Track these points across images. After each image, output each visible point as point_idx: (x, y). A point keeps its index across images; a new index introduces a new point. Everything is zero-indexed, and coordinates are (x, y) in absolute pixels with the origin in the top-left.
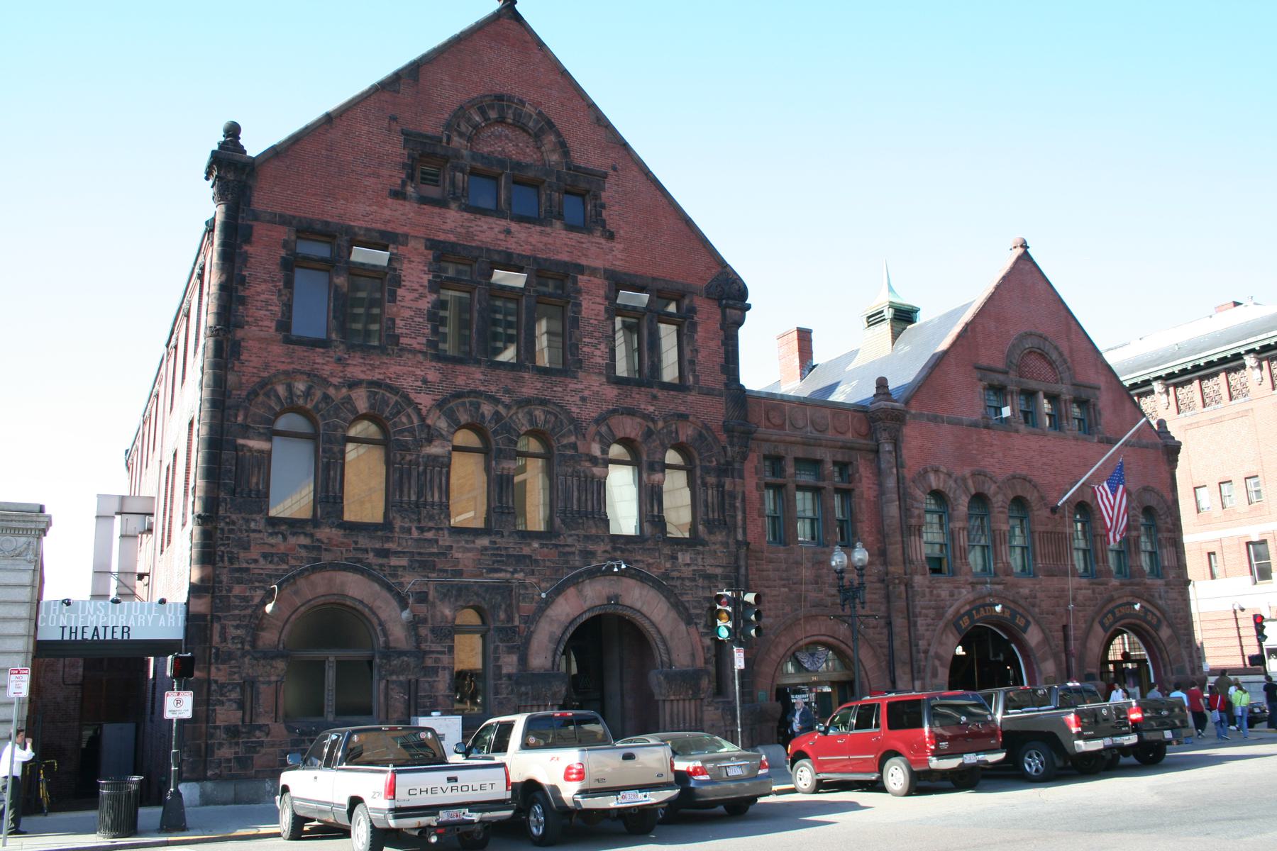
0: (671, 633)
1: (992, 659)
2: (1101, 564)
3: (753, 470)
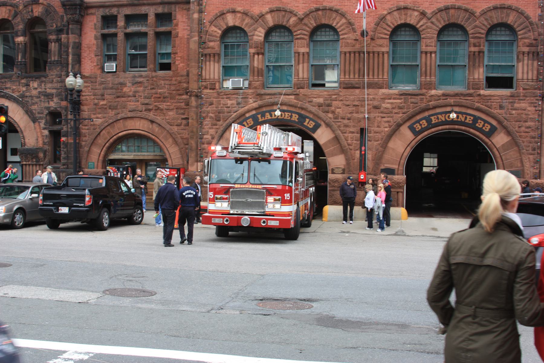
0: (25, 127)
2: (428, 78)
3: (93, 27)
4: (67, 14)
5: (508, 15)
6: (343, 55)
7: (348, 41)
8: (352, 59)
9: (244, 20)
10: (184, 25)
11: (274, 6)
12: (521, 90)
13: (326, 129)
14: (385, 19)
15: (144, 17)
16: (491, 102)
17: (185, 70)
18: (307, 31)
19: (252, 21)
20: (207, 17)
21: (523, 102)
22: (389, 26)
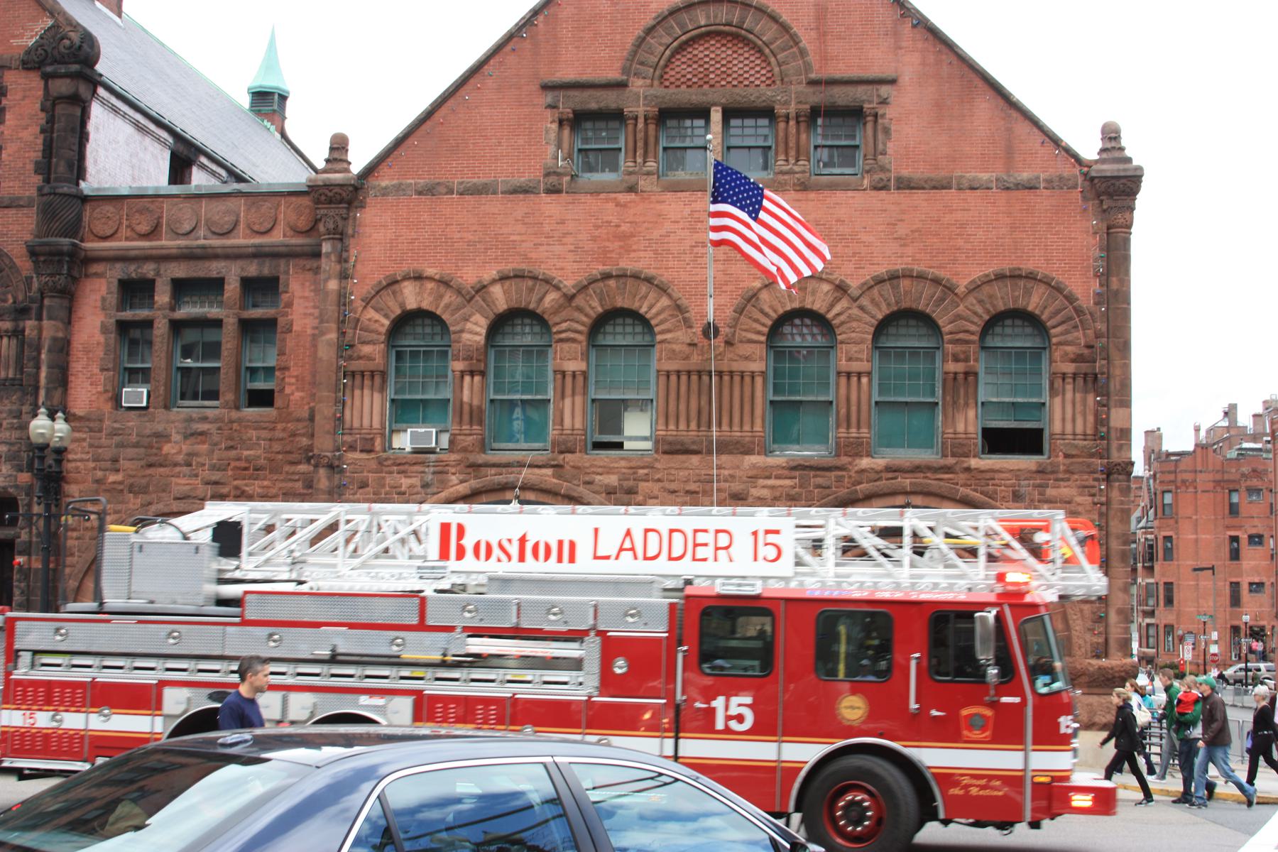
2: (853, 430)
3: (99, 304)
4: (39, 274)
5: (1028, 293)
6: (663, 379)
7: (674, 346)
8: (683, 388)
9: (441, 297)
10: (307, 304)
11: (509, 267)
12: (1061, 459)
15: (216, 285)
16: (993, 485)
17: (306, 407)
18: (583, 324)
19: (460, 299)
20: (358, 289)
21: (1066, 484)
22: (766, 315)
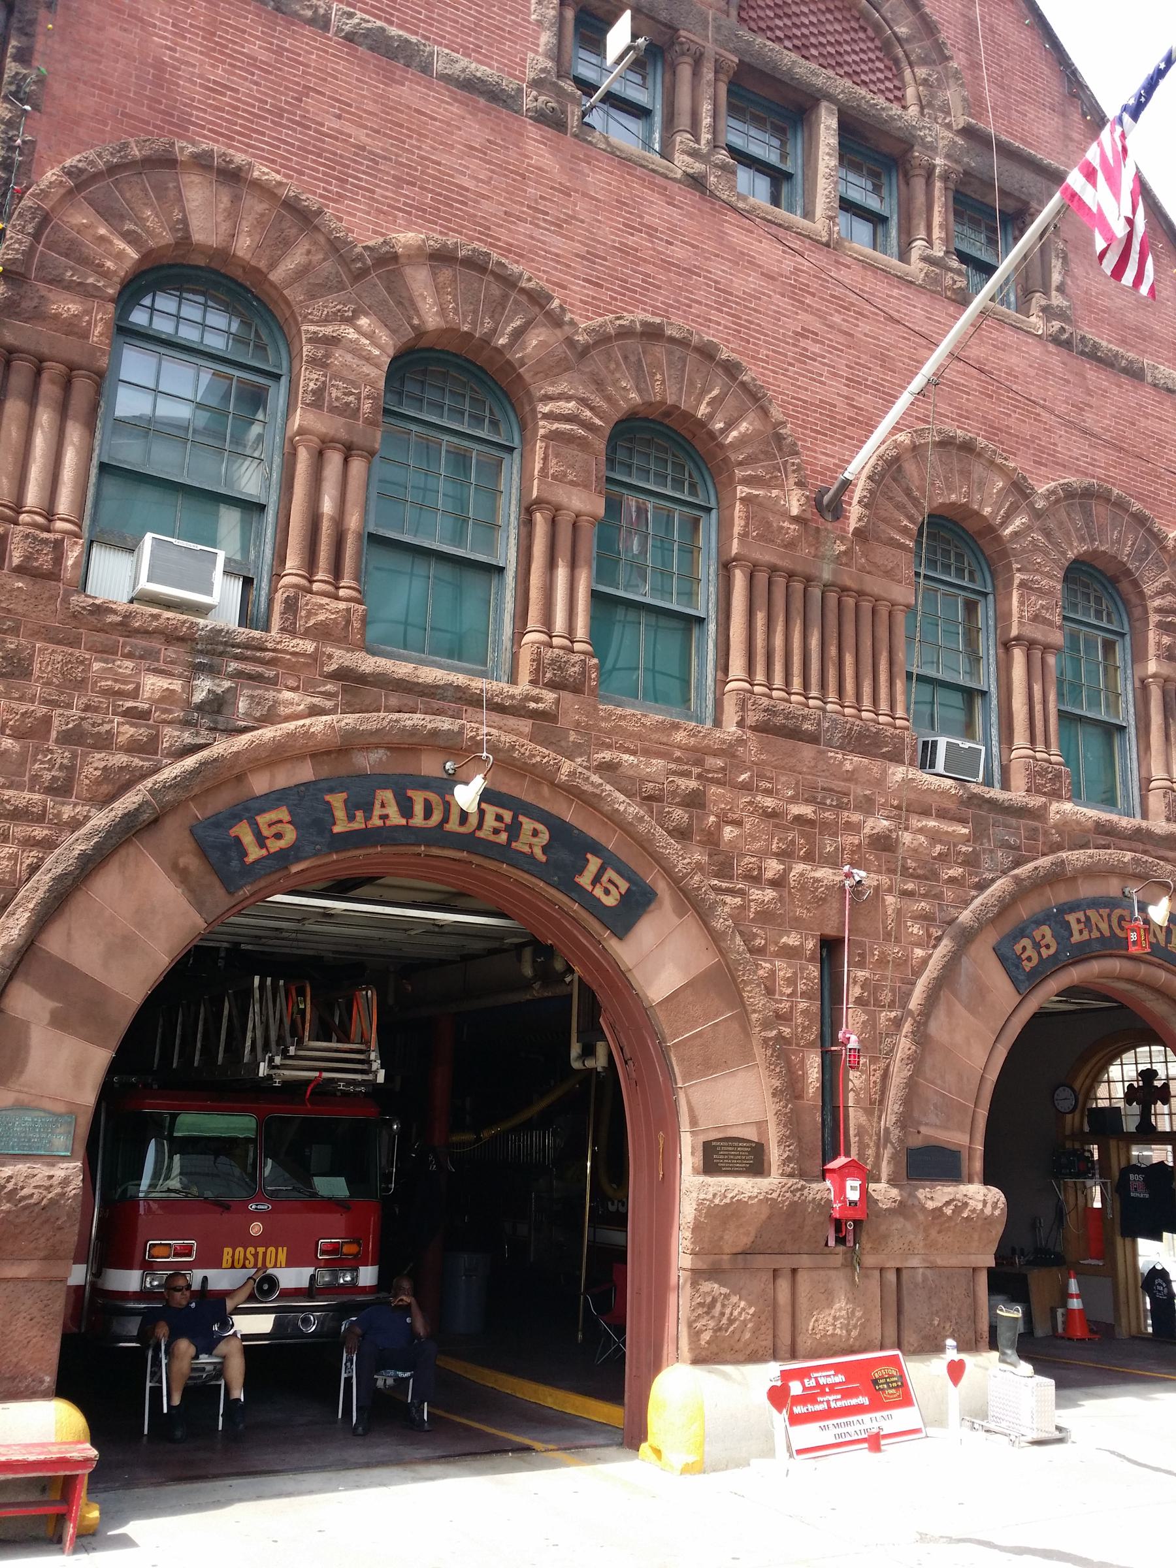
1: (576, 1065)
13: (676, 921)
14: (900, 467)
19: (329, 267)
